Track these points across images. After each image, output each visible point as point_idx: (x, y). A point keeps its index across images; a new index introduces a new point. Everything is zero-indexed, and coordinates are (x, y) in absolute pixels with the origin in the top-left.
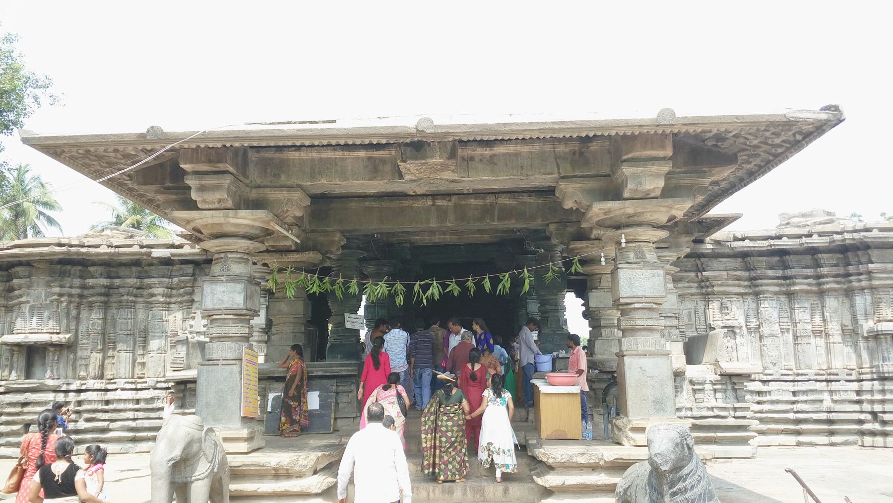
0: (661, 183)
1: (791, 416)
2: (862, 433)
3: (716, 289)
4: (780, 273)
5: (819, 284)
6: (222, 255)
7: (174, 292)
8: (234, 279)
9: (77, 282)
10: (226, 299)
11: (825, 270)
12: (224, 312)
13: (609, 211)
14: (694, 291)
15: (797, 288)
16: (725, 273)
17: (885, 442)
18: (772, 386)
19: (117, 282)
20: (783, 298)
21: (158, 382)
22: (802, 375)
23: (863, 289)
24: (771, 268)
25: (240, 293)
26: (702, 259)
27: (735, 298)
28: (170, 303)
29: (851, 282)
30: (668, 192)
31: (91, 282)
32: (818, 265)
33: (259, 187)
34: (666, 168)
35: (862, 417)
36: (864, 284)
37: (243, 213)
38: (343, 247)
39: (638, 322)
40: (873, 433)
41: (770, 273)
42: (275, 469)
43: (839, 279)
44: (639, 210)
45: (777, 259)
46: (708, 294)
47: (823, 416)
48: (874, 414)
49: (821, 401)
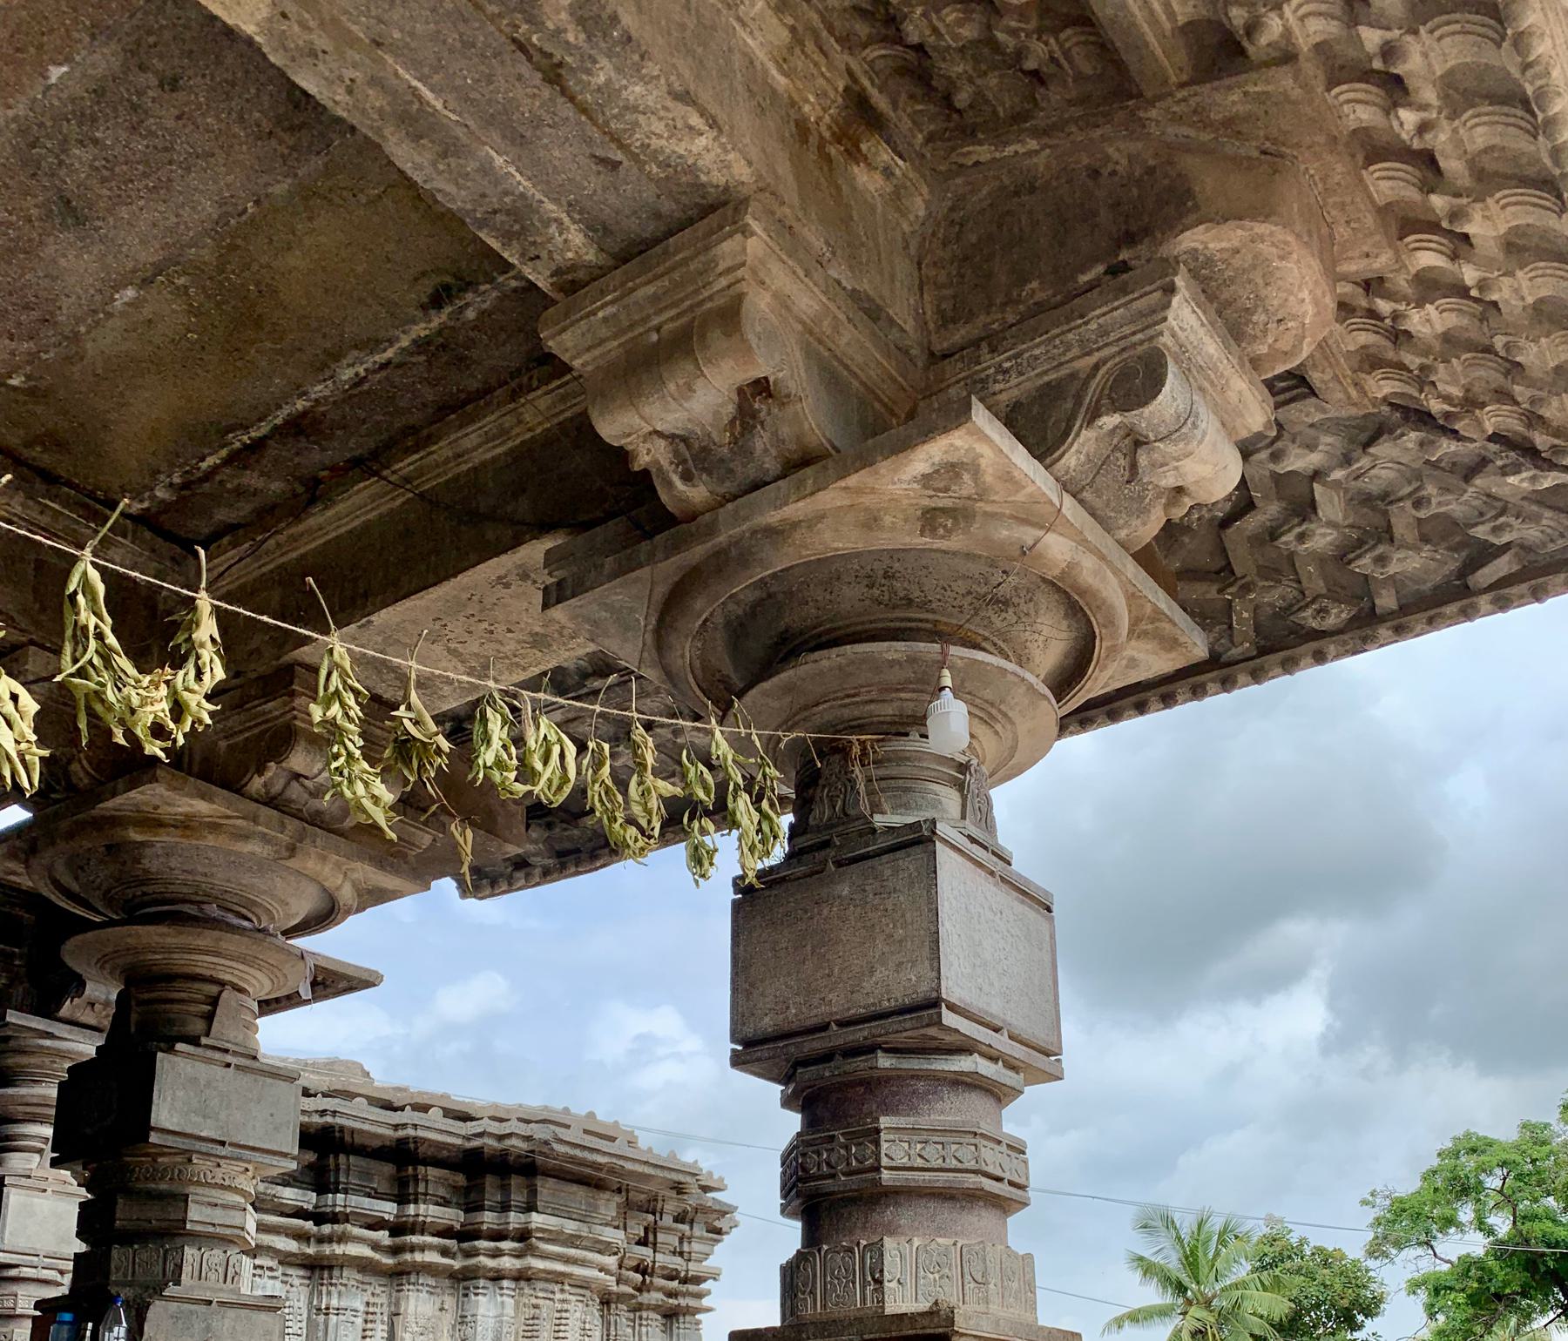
15: (353, 1250)
23: (497, 1277)
36: (507, 1263)
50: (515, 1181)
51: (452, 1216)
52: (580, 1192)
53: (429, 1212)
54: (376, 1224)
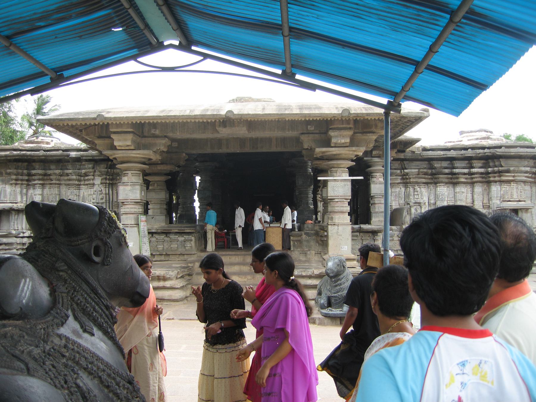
3: (411, 180)
5: (472, 178)
7: (82, 178)
14: (399, 181)
28: (80, 185)
31: (34, 172)
34: (350, 133)
36: (497, 179)
39: (336, 208)
42: (158, 276)
43: (484, 176)
46: (407, 183)
50: (495, 160)
54: (465, 174)
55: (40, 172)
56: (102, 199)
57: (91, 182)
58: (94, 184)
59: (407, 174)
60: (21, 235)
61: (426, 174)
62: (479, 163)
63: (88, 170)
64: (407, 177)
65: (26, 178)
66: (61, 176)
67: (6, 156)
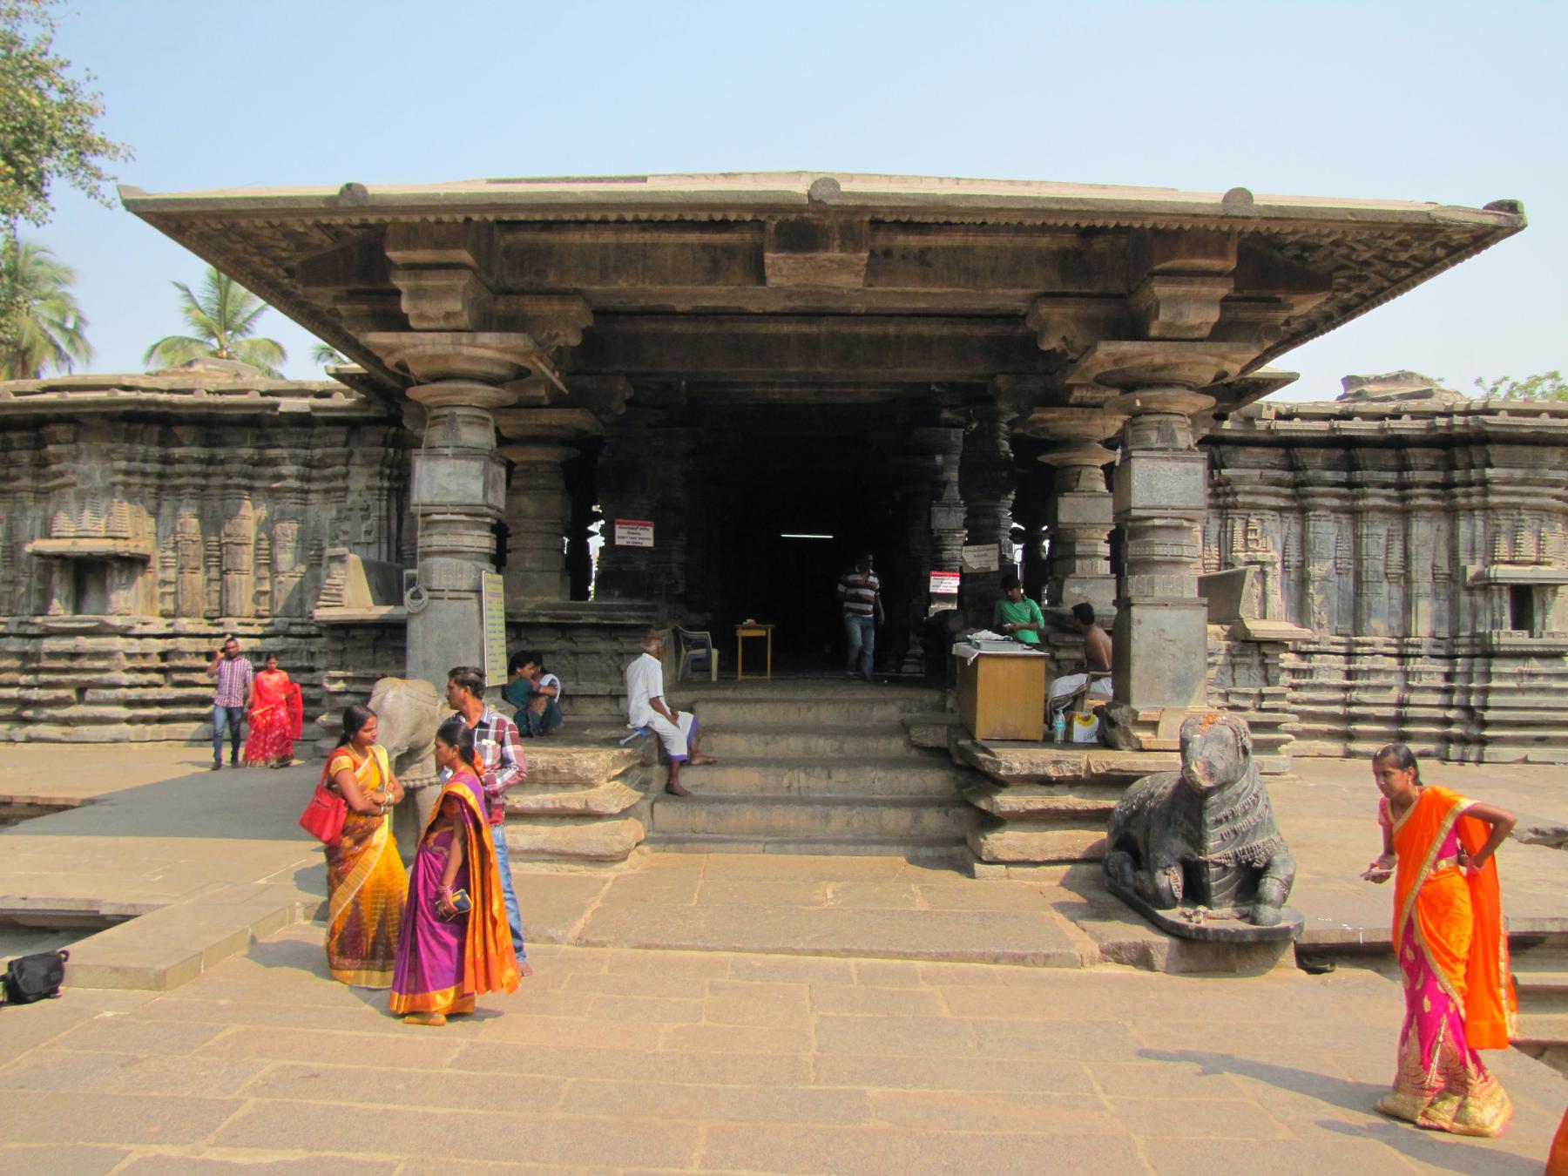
0: (1213, 315)
1: (1338, 709)
2: (1447, 739)
3: (1240, 499)
4: (1342, 476)
5: (1403, 499)
6: (445, 411)
7: (315, 473)
8: (468, 453)
9: (156, 451)
10: (452, 487)
11: (1417, 475)
12: (451, 509)
13: (1123, 358)
15: (1370, 502)
16: (1257, 472)
17: (1481, 754)
18: (1316, 662)
19: (221, 453)
20: (1344, 518)
21: (291, 624)
22: (1364, 644)
23: (1471, 510)
24: (1329, 469)
25: (476, 477)
26: (1223, 449)
27: (1268, 515)
28: (308, 492)
29: (1454, 496)
30: (1220, 332)
31: (177, 452)
32: (1404, 467)
33: (509, 292)
34: (1222, 290)
35: (1452, 714)
36: (1475, 500)
37: (485, 337)
38: (629, 403)
40: (1464, 740)
41: (1329, 475)
44: (1174, 359)
45: (1340, 452)
46: (1227, 507)
47: (1390, 712)
48: (1468, 709)
49: (1390, 688)
50: (1474, 450)
51: (1437, 477)
52: (1528, 450)
53: (1417, 475)
55: (197, 452)
56: (368, 532)
57: (339, 483)
58: (346, 489)
59: (1228, 482)
60: (139, 629)
61: (1278, 483)
62: (1428, 456)
63: (329, 450)
64: (1228, 489)
65: (157, 467)
66: (256, 464)
67: (97, 403)
